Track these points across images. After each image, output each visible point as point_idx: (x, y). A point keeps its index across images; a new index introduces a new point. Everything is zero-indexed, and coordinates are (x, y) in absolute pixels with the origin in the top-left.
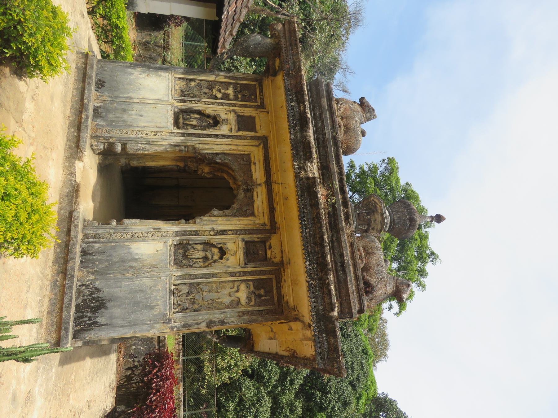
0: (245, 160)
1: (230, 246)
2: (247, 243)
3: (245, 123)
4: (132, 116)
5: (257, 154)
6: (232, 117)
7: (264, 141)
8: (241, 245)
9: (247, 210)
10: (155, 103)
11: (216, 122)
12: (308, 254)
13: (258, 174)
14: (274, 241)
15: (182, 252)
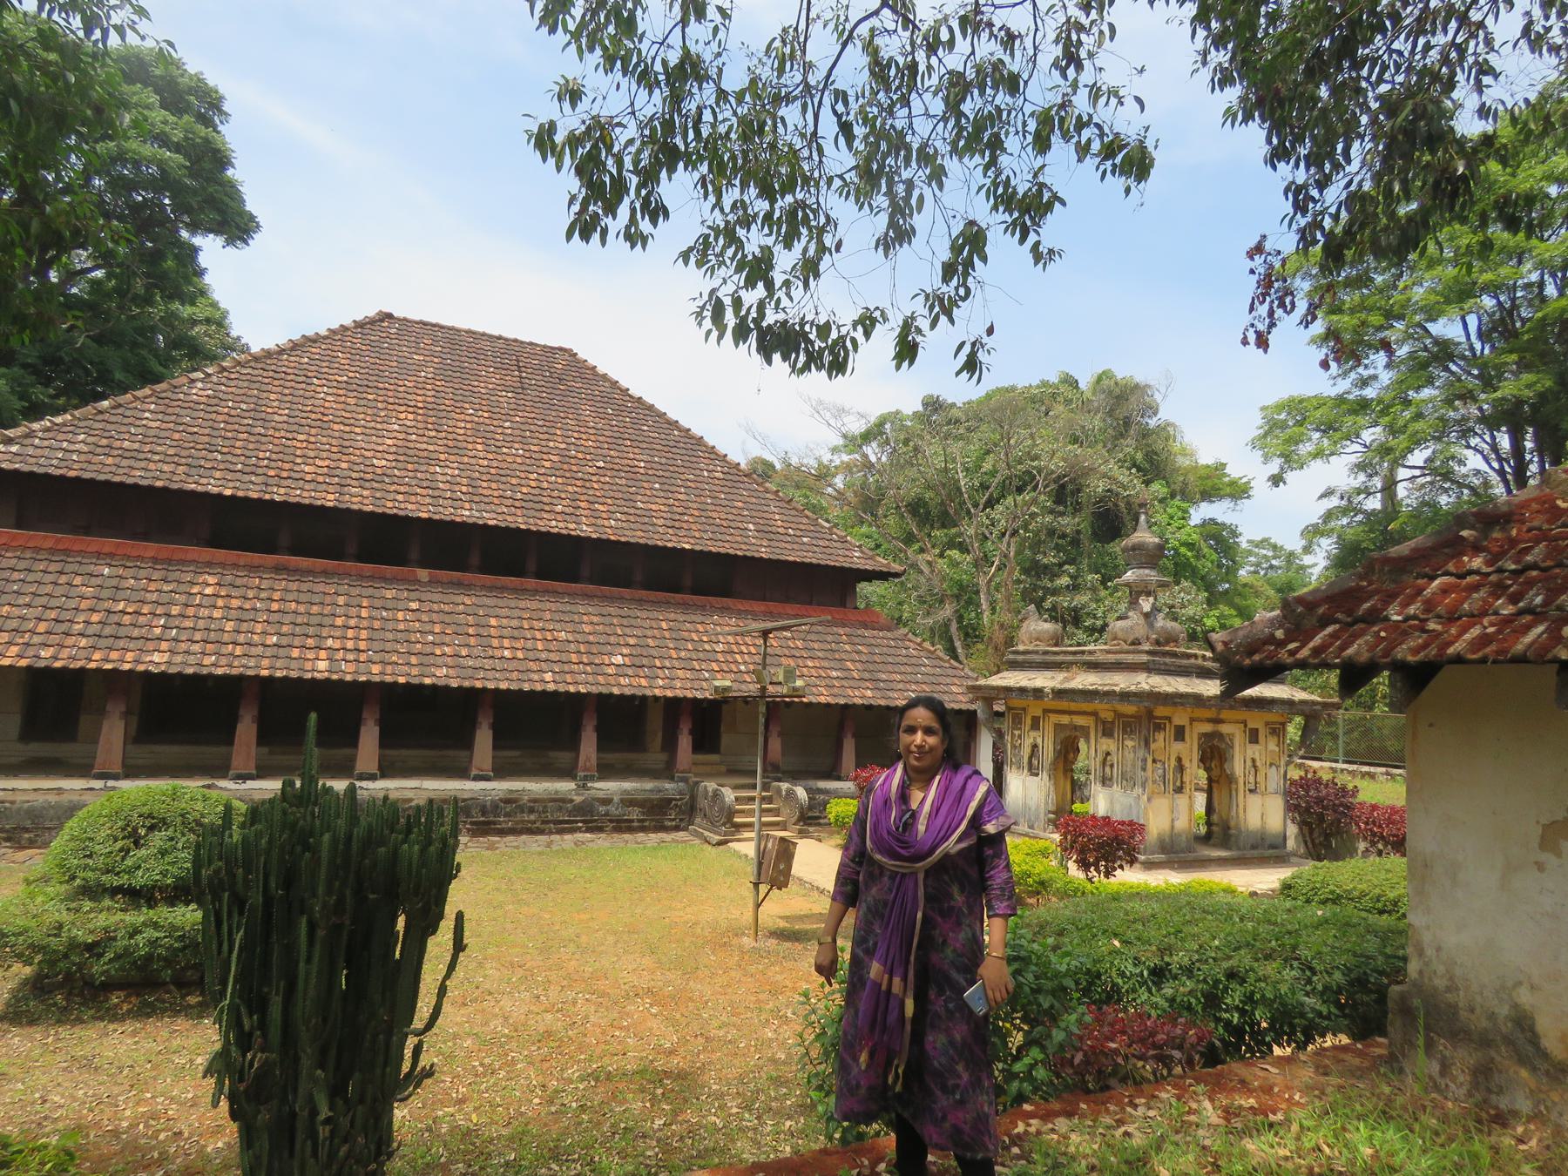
0: (1058, 727)
1: (1105, 747)
2: (1104, 734)
3: (1035, 725)
4: (1032, 803)
5: (1054, 718)
6: (1033, 734)
7: (1046, 711)
8: (1104, 740)
9: (1085, 731)
10: (1025, 788)
11: (1035, 746)
12: (1091, 701)
13: (1065, 719)
14: (1102, 715)
15: (1105, 781)
